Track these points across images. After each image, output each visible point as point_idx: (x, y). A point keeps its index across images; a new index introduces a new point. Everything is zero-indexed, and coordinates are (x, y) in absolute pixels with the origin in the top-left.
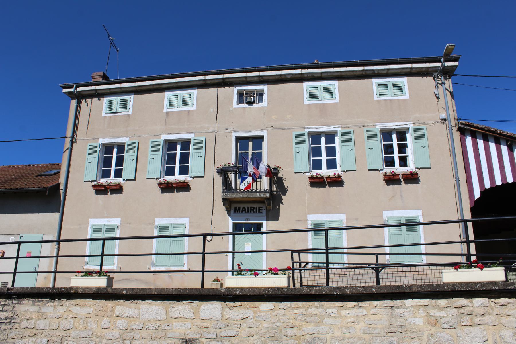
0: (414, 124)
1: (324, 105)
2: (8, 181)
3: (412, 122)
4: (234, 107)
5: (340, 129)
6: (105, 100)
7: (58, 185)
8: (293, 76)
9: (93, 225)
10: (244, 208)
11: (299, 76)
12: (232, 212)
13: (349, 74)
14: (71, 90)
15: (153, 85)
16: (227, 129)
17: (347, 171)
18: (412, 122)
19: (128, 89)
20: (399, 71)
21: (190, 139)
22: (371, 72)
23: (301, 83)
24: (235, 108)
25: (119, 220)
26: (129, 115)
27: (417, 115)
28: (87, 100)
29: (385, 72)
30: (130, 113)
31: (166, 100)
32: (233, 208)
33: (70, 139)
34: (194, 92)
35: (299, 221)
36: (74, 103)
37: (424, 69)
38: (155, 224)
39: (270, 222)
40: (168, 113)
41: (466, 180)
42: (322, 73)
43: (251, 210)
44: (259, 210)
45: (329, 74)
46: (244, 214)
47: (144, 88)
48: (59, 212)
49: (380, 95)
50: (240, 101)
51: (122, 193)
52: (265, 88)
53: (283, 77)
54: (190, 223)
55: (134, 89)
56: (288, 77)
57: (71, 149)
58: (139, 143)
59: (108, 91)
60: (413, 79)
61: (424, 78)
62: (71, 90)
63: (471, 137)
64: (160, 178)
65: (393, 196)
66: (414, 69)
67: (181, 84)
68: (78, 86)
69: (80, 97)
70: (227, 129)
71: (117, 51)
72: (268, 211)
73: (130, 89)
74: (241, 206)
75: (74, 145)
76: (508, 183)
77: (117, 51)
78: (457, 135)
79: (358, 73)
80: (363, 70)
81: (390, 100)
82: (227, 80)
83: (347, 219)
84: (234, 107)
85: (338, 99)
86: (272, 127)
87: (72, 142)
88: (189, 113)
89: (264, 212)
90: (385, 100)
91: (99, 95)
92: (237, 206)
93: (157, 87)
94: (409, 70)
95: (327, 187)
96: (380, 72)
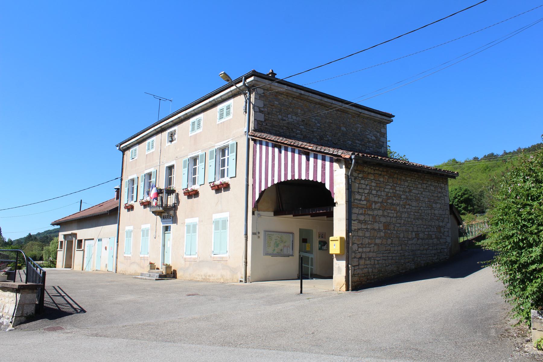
3: (231, 139)
13: (205, 106)
15: (141, 138)
25: (132, 226)
26: (136, 159)
32: (162, 217)
35: (182, 223)
38: (142, 229)
39: (173, 224)
51: (198, 197)
56: (182, 118)
65: (218, 202)
66: (233, 92)
68: (121, 145)
69: (124, 151)
71: (170, 101)
77: (170, 101)
81: (223, 122)
83: (199, 221)
88: (153, 153)
89: (171, 217)
90: (221, 123)
91: (128, 148)
93: (142, 138)
94: (230, 93)
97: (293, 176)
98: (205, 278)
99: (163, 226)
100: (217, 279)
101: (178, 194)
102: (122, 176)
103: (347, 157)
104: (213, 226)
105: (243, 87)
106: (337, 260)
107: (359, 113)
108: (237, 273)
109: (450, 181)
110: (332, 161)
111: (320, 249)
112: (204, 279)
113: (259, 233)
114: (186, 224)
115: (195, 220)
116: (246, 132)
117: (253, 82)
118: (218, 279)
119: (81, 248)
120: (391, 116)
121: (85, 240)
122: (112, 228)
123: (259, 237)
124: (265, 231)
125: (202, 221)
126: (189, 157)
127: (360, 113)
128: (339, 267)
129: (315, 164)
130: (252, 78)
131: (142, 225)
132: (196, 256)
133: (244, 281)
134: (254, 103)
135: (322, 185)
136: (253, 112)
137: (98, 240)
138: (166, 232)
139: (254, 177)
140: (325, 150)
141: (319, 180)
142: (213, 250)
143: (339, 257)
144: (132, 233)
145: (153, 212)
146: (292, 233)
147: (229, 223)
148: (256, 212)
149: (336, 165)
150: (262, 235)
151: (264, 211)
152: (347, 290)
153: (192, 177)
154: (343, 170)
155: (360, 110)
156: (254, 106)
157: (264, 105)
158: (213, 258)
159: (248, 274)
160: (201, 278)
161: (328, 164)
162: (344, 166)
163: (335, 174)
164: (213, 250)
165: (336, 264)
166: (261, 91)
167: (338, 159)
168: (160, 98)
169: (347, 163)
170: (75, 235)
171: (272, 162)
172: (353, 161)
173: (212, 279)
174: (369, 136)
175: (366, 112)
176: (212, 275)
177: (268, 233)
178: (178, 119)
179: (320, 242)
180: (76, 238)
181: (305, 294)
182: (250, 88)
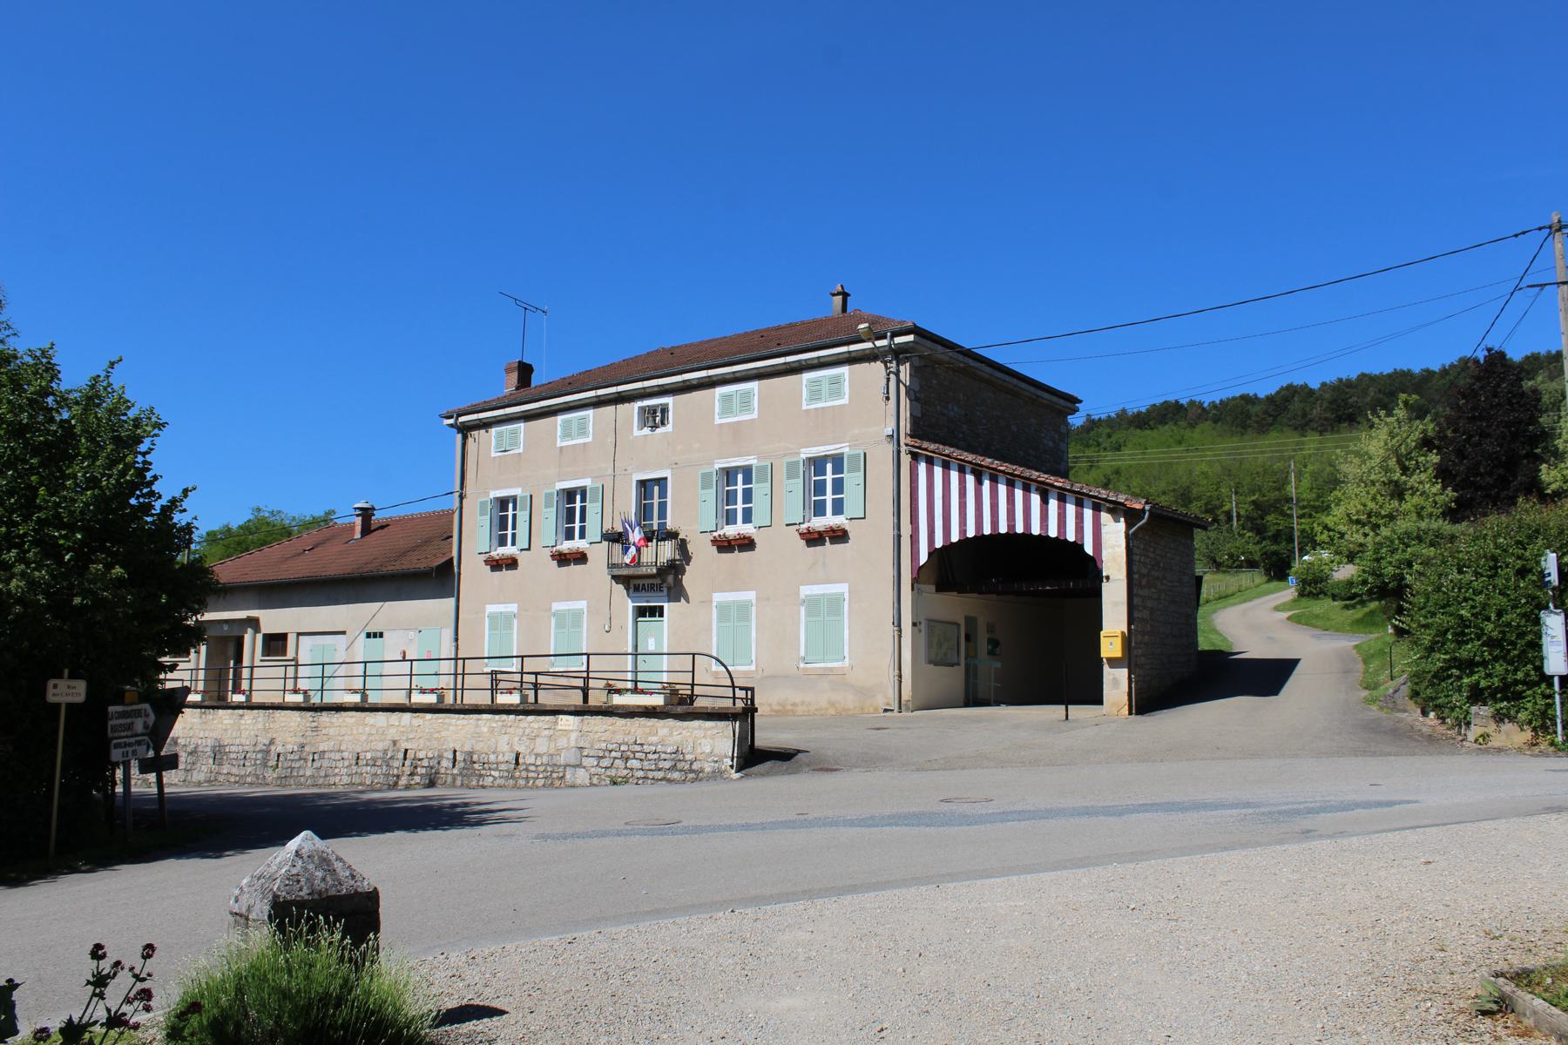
0: (850, 446)
1: (738, 423)
2: (404, 554)
3: (848, 444)
4: (635, 435)
5: (756, 461)
6: (494, 431)
7: (452, 559)
8: (701, 381)
9: (490, 613)
10: (644, 585)
11: (707, 380)
12: (631, 590)
13: (769, 370)
14: (451, 421)
16: (626, 470)
17: (760, 527)
18: (848, 444)
19: (515, 415)
20: (834, 358)
21: (586, 487)
22: (797, 365)
23: (712, 390)
24: (636, 437)
25: (516, 605)
26: (519, 454)
27: (856, 431)
28: (473, 433)
29: (816, 361)
30: (521, 450)
31: (559, 428)
32: (632, 586)
33: (458, 494)
34: (590, 413)
36: (459, 436)
37: (867, 352)
38: (553, 610)
39: (671, 603)
40: (561, 448)
41: (911, 536)
42: (734, 372)
43: (652, 588)
44: (660, 587)
45: (744, 373)
46: (643, 594)
47: (531, 412)
48: (453, 596)
49: (811, 400)
50: (643, 424)
52: (667, 400)
53: (688, 383)
54: (588, 607)
55: (522, 414)
56: (695, 382)
57: (461, 508)
58: (531, 496)
59: (494, 420)
60: (857, 366)
61: (873, 363)
62: (451, 421)
63: (926, 463)
64: (555, 546)
67: (572, 404)
68: (460, 415)
69: (465, 430)
70: (626, 470)
72: (669, 589)
73: (518, 415)
74: (641, 582)
75: (464, 501)
76: (967, 538)
78: (906, 460)
79: (780, 368)
80: (785, 363)
81: (823, 408)
82: (623, 394)
84: (635, 435)
85: (756, 412)
86: (676, 464)
87: (462, 497)
89: (665, 590)
90: (816, 409)
91: (486, 425)
92: (637, 582)
93: (547, 409)
94: (847, 355)
95: (736, 552)
96: (809, 362)
97: (995, 522)
98: (781, 708)
99: (633, 607)
100: (817, 710)
101: (684, 542)
102: (462, 488)
103: (1138, 506)
104: (803, 609)
105: (887, 348)
106: (1111, 667)
107: (1035, 397)
108: (874, 696)
109: (1199, 534)
110: (1097, 508)
111: (991, 653)
112: (777, 711)
113: (920, 623)
114: (714, 604)
115: (751, 596)
116: (892, 436)
117: (910, 344)
118: (821, 709)
119: (285, 655)
120: (1075, 400)
121: (299, 634)
122: (442, 607)
123: (920, 631)
124: (929, 621)
125: (768, 599)
126: (717, 466)
127: (1038, 396)
128: (1114, 679)
129: (1061, 511)
130: (911, 338)
131: (553, 604)
132: (753, 668)
133: (896, 709)
134: (908, 384)
135: (1078, 547)
136: (908, 401)
137: (363, 635)
138: (640, 619)
139: (913, 521)
140: (1090, 491)
141: (1071, 537)
142: (802, 653)
143: (1114, 663)
144: (515, 622)
145: (614, 577)
146: (958, 625)
147: (850, 606)
148: (915, 585)
149: (1105, 517)
150: (923, 627)
151: (924, 584)
152: (1130, 713)
153: (723, 508)
154: (1122, 525)
155: (1039, 393)
156: (910, 389)
157: (921, 387)
158: (805, 669)
159: (904, 698)
160: (769, 709)
161: (1088, 513)
162: (1122, 519)
163: (1104, 530)
164: (802, 653)
165: (1109, 673)
166: (917, 362)
167: (1116, 509)
168: (526, 306)
169: (1131, 516)
170: (254, 623)
171: (960, 498)
172: (1147, 514)
173: (800, 709)
174: (1045, 441)
175: (1047, 396)
176: (803, 703)
177: (932, 623)
178: (682, 384)
179: (990, 641)
180: (257, 629)
181: (1073, 721)
182: (899, 354)
